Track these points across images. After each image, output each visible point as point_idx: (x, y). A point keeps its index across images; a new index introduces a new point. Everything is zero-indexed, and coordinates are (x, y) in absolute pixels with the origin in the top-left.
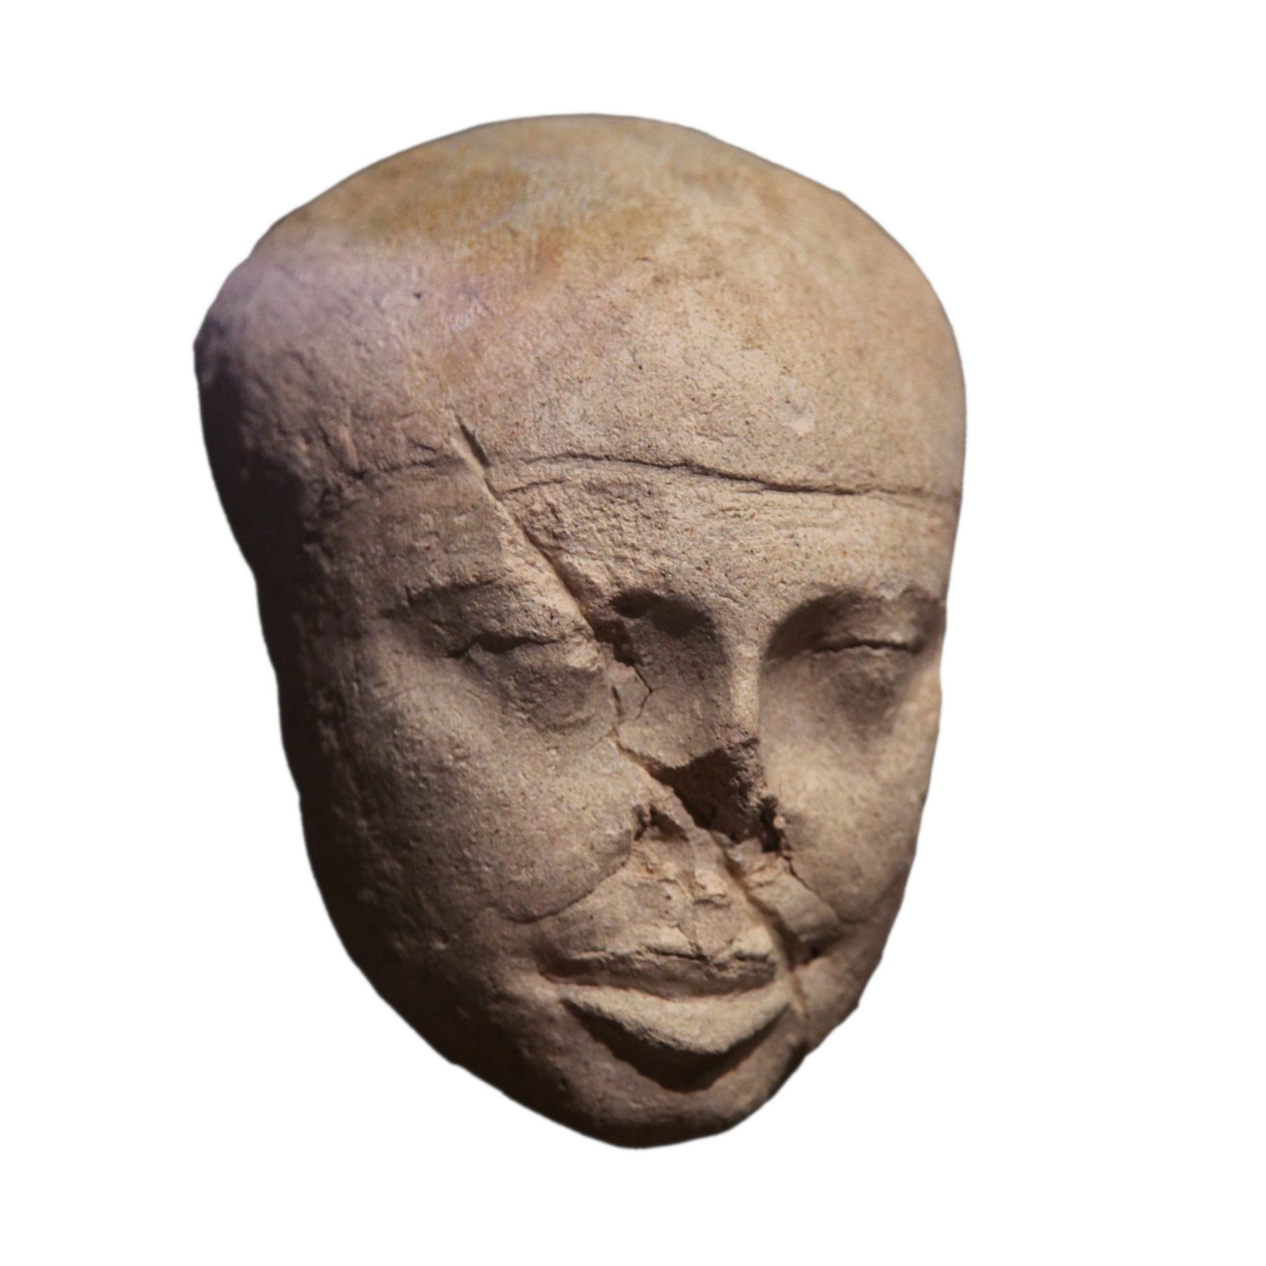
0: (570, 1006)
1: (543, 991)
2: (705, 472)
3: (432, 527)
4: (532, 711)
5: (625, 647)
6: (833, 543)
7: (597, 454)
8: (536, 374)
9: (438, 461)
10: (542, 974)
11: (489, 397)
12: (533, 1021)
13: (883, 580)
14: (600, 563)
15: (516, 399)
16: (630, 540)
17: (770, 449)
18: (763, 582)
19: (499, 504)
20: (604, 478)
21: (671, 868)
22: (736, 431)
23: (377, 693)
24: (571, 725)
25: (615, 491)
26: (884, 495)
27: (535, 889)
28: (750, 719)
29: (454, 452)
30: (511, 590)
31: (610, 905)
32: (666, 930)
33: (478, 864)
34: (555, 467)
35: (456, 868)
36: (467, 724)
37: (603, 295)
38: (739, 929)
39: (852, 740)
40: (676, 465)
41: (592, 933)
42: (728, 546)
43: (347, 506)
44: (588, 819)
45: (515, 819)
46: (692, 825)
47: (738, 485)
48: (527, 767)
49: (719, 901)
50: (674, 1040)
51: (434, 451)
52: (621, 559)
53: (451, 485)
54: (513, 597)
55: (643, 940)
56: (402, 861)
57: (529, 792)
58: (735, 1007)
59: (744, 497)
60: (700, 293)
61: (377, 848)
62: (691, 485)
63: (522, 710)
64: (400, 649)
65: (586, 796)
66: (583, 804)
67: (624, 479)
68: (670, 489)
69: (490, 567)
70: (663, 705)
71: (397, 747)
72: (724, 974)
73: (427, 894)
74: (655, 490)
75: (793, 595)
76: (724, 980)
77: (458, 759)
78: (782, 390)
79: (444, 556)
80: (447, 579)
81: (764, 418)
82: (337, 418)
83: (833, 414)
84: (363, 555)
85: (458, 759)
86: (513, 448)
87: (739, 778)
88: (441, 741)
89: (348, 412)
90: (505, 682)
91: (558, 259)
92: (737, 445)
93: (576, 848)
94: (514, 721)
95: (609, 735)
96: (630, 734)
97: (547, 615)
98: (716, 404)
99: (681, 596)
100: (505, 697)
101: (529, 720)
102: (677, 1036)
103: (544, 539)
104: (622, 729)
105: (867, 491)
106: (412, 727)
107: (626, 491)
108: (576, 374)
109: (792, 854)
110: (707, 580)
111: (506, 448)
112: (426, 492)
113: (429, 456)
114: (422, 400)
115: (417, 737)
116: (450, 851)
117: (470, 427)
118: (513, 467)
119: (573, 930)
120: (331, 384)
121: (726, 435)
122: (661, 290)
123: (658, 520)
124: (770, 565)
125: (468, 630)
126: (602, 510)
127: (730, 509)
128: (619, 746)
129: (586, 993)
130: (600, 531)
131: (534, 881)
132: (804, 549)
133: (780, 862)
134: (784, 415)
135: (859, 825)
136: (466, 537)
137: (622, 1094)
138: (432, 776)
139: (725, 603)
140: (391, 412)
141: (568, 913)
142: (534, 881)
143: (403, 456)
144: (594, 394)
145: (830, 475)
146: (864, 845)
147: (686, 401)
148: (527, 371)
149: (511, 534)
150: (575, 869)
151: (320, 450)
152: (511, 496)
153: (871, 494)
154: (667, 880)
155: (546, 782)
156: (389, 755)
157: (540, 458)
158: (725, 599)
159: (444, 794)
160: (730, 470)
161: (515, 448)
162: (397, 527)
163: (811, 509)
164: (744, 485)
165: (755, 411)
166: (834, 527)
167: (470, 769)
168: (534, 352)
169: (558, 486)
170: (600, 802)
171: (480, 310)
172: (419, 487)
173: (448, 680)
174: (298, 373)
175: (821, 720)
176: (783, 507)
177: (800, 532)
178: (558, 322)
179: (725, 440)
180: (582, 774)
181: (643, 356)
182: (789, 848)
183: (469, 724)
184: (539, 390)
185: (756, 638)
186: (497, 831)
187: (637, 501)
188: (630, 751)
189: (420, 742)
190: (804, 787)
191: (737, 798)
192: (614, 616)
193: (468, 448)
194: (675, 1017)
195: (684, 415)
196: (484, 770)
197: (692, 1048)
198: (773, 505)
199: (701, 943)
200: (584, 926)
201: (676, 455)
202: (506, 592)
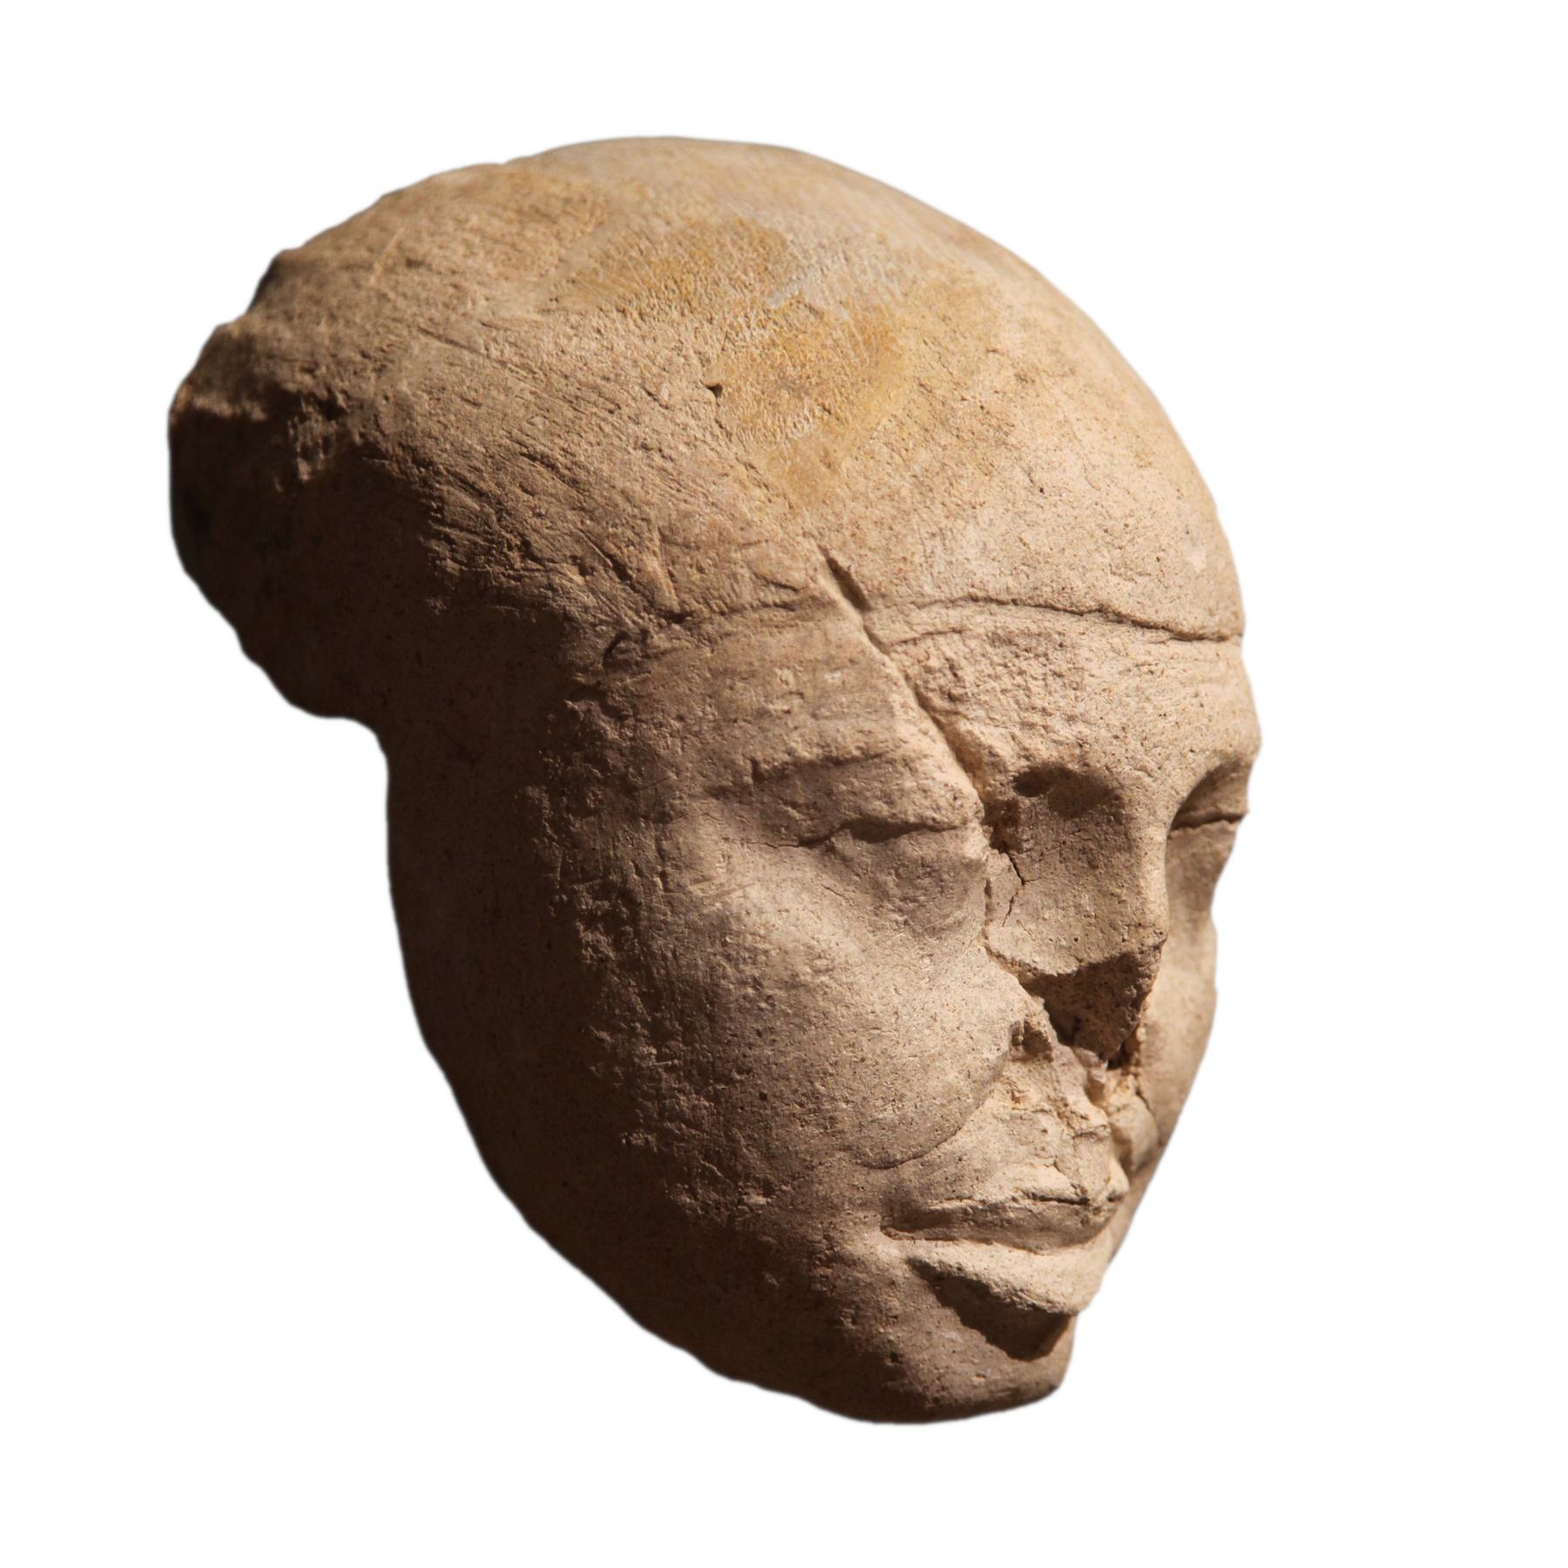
0: (920, 1268)
1: (884, 1250)
2: (1120, 619)
3: (793, 686)
8: (918, 497)
9: (801, 602)
11: (862, 523)
16: (1039, 703)
18: (1175, 752)
19: (886, 658)
20: (1012, 627)
22: (1149, 569)
23: (696, 890)
25: (1022, 642)
29: (823, 593)
34: (952, 612)
35: (801, 1105)
36: (828, 929)
41: (959, 1178)
43: (660, 655)
45: (885, 1044)
47: (1150, 634)
48: (900, 980)
50: (1048, 1301)
51: (795, 590)
52: (1027, 726)
53: (817, 633)
54: (907, 774)
55: (1018, 1184)
56: (715, 1098)
57: (903, 1011)
61: (668, 1081)
63: (900, 910)
67: (1034, 628)
68: (1085, 641)
69: (881, 737)
70: (1037, 900)
71: (728, 958)
73: (750, 1137)
74: (1068, 642)
77: (817, 972)
79: (810, 721)
80: (816, 750)
82: (641, 546)
84: (680, 718)
85: (817, 972)
89: (656, 536)
90: (882, 877)
93: (953, 1076)
96: (1003, 936)
97: (949, 795)
99: (1097, 770)
100: (880, 893)
101: (906, 922)
102: (1052, 1297)
103: (938, 701)
107: (1034, 644)
108: (967, 497)
109: (1140, 1070)
112: (783, 642)
113: (786, 596)
114: (767, 523)
116: (795, 1085)
117: (843, 562)
120: (619, 499)
121: (1140, 574)
123: (1070, 677)
125: (833, 814)
126: (1006, 666)
128: (988, 950)
129: (940, 1250)
130: (1004, 691)
137: (967, 1368)
138: (780, 993)
139: (1139, 778)
140: (725, 538)
143: (747, 593)
147: (1099, 533)
148: (904, 492)
149: (902, 697)
151: (608, 582)
152: (899, 649)
155: (921, 995)
159: (795, 1015)
162: (739, 685)
167: (834, 985)
168: (908, 468)
169: (956, 637)
170: (974, 1020)
172: (771, 634)
173: (799, 874)
177: (1202, 689)
179: (1139, 579)
180: (953, 987)
183: (831, 929)
186: (863, 1060)
187: (1046, 655)
188: (999, 956)
189: (766, 952)
191: (1126, 1010)
195: (1097, 550)
196: (850, 986)
199: (1086, 1184)
200: (951, 1170)
201: (1093, 599)
202: (900, 768)
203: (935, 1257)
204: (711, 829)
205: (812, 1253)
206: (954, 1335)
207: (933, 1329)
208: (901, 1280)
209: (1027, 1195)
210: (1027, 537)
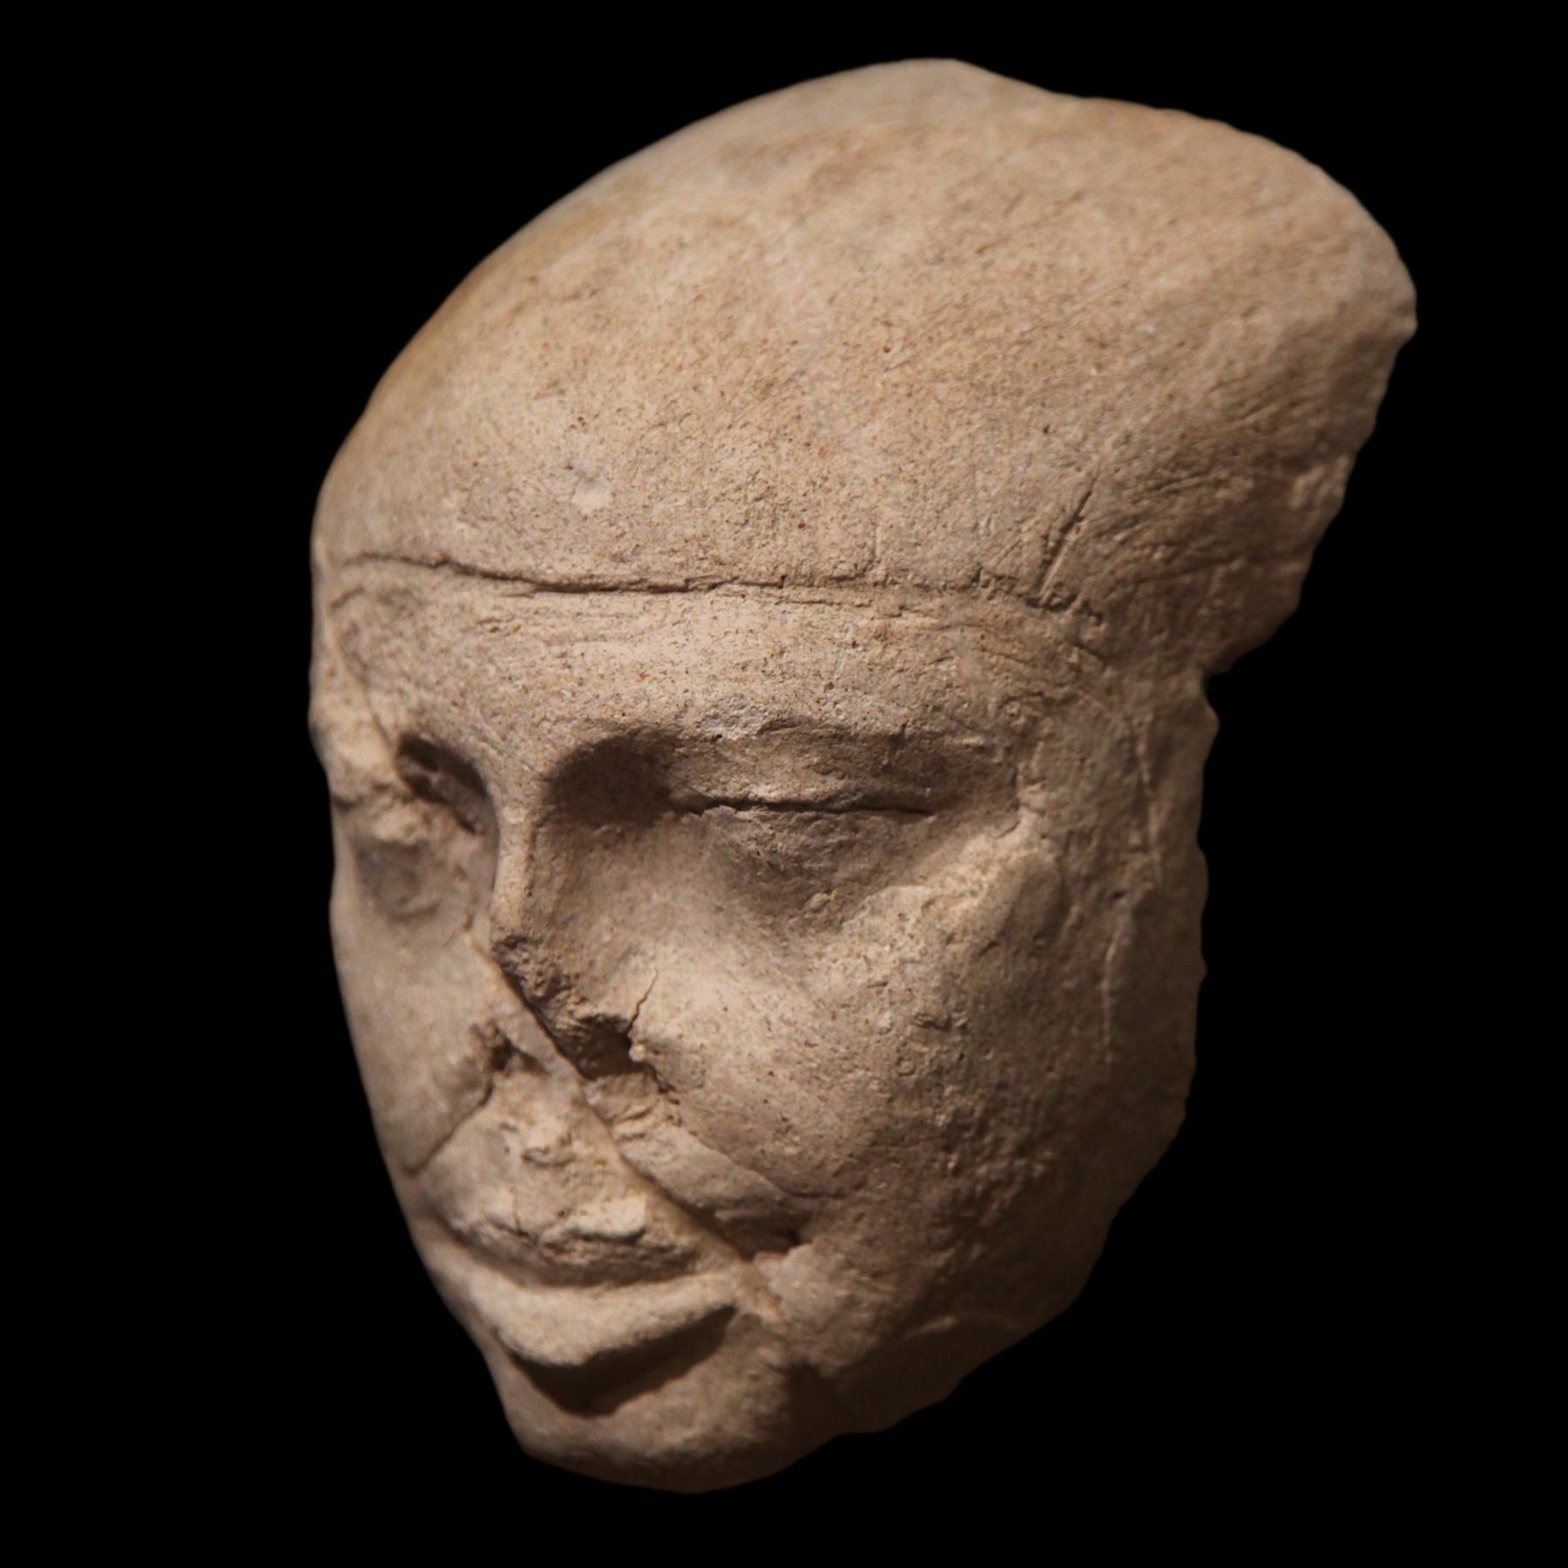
2: (466, 571)
6: (626, 662)
13: (712, 712)
17: (537, 534)
22: (496, 512)
26: (751, 590)
39: (763, 937)
42: (485, 671)
72: (564, 1258)
75: (561, 737)
76: (566, 1266)
78: (563, 451)
81: (530, 491)
83: (653, 479)
105: (713, 586)
121: (485, 519)
124: (531, 695)
127: (489, 620)
134: (561, 486)
135: (779, 1058)
139: (483, 750)
147: (452, 475)
153: (721, 591)
158: (484, 745)
163: (602, 616)
165: (519, 484)
175: (719, 909)
176: (560, 616)
179: (483, 525)
185: (521, 797)
190: (688, 1004)
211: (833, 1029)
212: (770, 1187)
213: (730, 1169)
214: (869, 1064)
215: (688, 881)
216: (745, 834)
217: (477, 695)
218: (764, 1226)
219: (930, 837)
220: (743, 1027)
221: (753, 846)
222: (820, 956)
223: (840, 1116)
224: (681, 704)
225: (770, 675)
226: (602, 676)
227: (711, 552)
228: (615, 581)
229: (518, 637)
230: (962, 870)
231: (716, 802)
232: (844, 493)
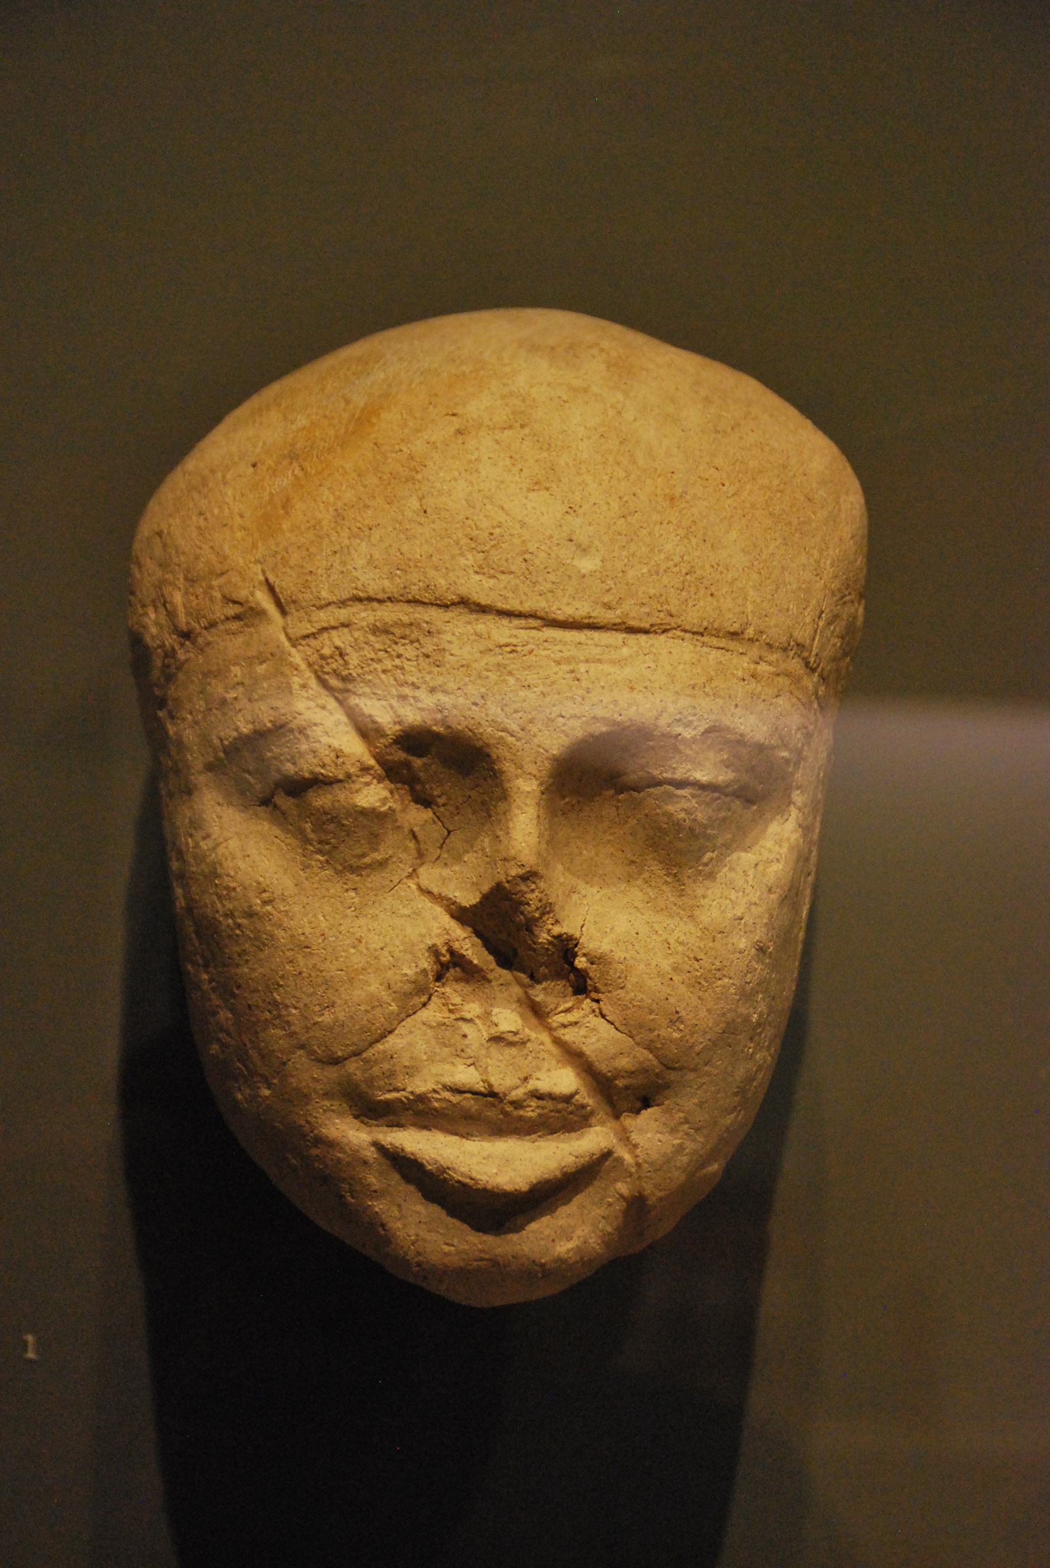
1: (355, 1135)
2: (483, 609)
4: (329, 853)
5: (418, 787)
7: (380, 596)
9: (245, 612)
10: (356, 1117)
11: (290, 549)
12: (349, 1164)
13: (678, 717)
14: (384, 703)
15: (313, 550)
16: (411, 679)
17: (549, 586)
19: (293, 651)
20: (387, 620)
21: (473, 1009)
22: (513, 568)
24: (367, 866)
25: (398, 632)
26: (688, 636)
27: (337, 1029)
28: (526, 852)
29: (258, 604)
30: (300, 732)
31: (410, 1044)
32: (461, 1067)
33: (287, 1007)
34: (343, 611)
35: (270, 1012)
37: (405, 449)
38: (539, 1069)
40: (454, 604)
41: (391, 1074)
44: (386, 959)
46: (493, 965)
47: (516, 622)
48: (327, 908)
49: (510, 1038)
50: (472, 1179)
52: (403, 698)
53: (255, 636)
54: (303, 740)
58: (538, 1148)
59: (523, 634)
60: (497, 442)
62: (469, 623)
63: (320, 852)
64: (221, 801)
65: (385, 937)
66: (382, 945)
67: (405, 619)
68: (448, 628)
69: (283, 711)
74: (433, 629)
75: (573, 729)
76: (520, 1118)
77: (265, 903)
78: (565, 528)
79: (248, 705)
80: (251, 726)
81: (542, 555)
83: (625, 553)
84: (191, 713)
86: (305, 595)
87: (522, 913)
88: (250, 885)
89: (181, 577)
91: (374, 420)
92: (514, 582)
93: (374, 987)
94: (314, 863)
95: (410, 876)
96: (430, 875)
98: (493, 543)
99: (459, 731)
102: (474, 1175)
103: (334, 682)
104: (421, 870)
106: (228, 875)
107: (408, 632)
110: (483, 715)
111: (300, 596)
115: (233, 885)
117: (272, 578)
118: (306, 613)
119: (376, 1071)
121: (503, 573)
122: (460, 441)
126: (386, 652)
127: (507, 645)
128: (420, 888)
129: (394, 1135)
131: (336, 1020)
132: (584, 684)
133: (587, 1004)
135: (676, 969)
136: (265, 685)
137: (433, 1236)
139: (502, 738)
141: (368, 1054)
142: (336, 1020)
144: (381, 540)
145: (618, 612)
146: (682, 989)
147: (464, 541)
148: (324, 522)
150: (373, 1008)
152: (303, 642)
153: (670, 634)
154: (463, 1019)
156: (213, 904)
157: (329, 604)
158: (502, 734)
160: (507, 607)
161: (308, 596)
164: (523, 622)
166: (621, 662)
167: (275, 912)
169: (346, 630)
170: (398, 943)
171: (297, 471)
173: (260, 828)
174: (158, 551)
175: (633, 862)
176: (565, 644)
178: (359, 475)
179: (502, 577)
180: (382, 916)
181: (430, 502)
182: (597, 990)
184: (333, 539)
185: (535, 772)
186: (300, 973)
187: (418, 641)
188: (429, 893)
189: (234, 889)
192: (401, 755)
193: (271, 601)
194: (472, 1155)
195: (462, 554)
197: (489, 1187)
198: (555, 642)
199: (492, 1080)
200: (386, 1066)
202: (297, 734)
203: (389, 1139)
204: (210, 797)
205: (304, 1136)
206: (419, 1208)
207: (402, 1202)
208: (371, 1161)
209: (445, 1087)
210: (405, 548)
211: (712, 949)
212: (655, 1062)
213: (632, 1049)
214: (732, 974)
215: (609, 841)
216: (679, 806)
217: (499, 698)
218: (625, 1093)
219: (753, 820)
220: (650, 946)
221: (682, 815)
222: (704, 897)
223: (709, 1011)
224: (660, 710)
225: (707, 695)
226: (603, 687)
227: (665, 607)
228: (605, 621)
229: (532, 658)
230: (769, 844)
231: (660, 783)
232: (730, 576)
